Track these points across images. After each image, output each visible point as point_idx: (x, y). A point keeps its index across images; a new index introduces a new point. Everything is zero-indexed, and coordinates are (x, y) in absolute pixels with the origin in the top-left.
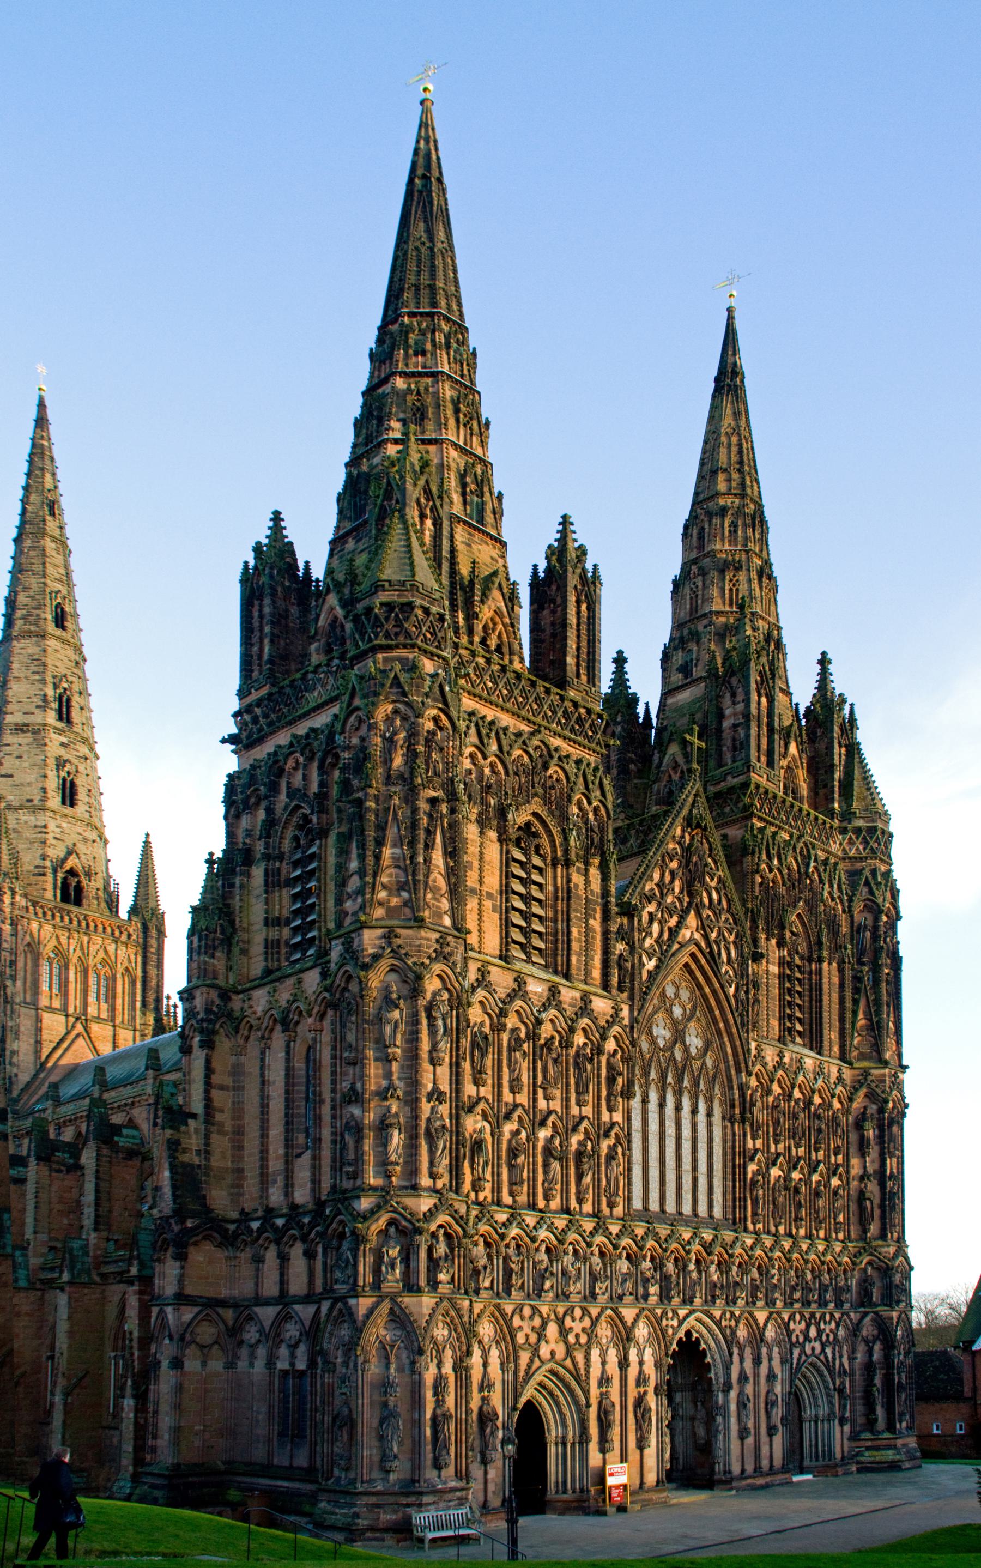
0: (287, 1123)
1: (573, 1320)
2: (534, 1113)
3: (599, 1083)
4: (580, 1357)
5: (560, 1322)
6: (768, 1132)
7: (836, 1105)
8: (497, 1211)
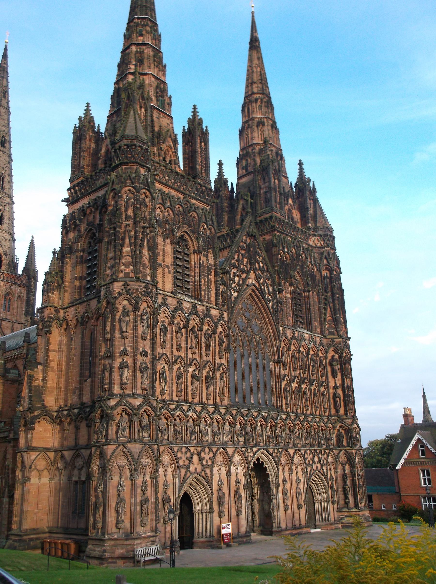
0: (81, 366)
1: (205, 454)
2: (187, 360)
3: (215, 346)
4: (208, 471)
5: (199, 454)
6: (290, 367)
7: (320, 354)
8: (170, 404)
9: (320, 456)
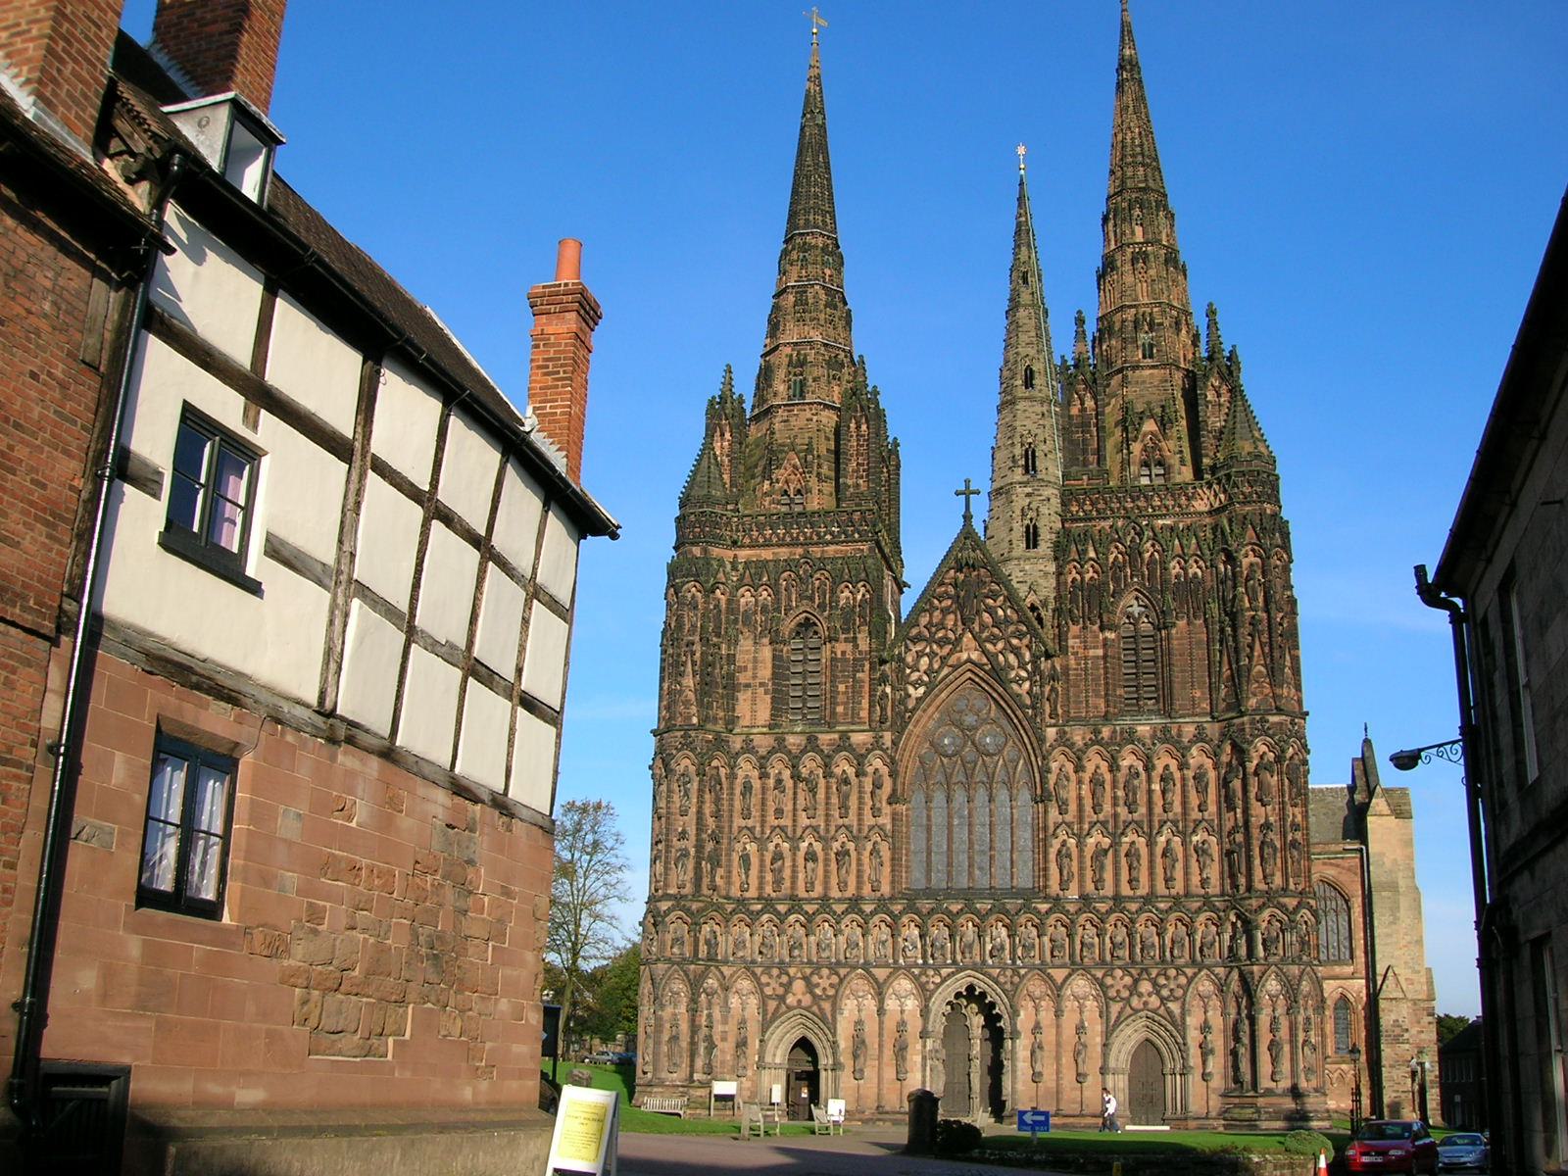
4: (827, 1006)
5: (806, 979)
9: (1162, 981)
